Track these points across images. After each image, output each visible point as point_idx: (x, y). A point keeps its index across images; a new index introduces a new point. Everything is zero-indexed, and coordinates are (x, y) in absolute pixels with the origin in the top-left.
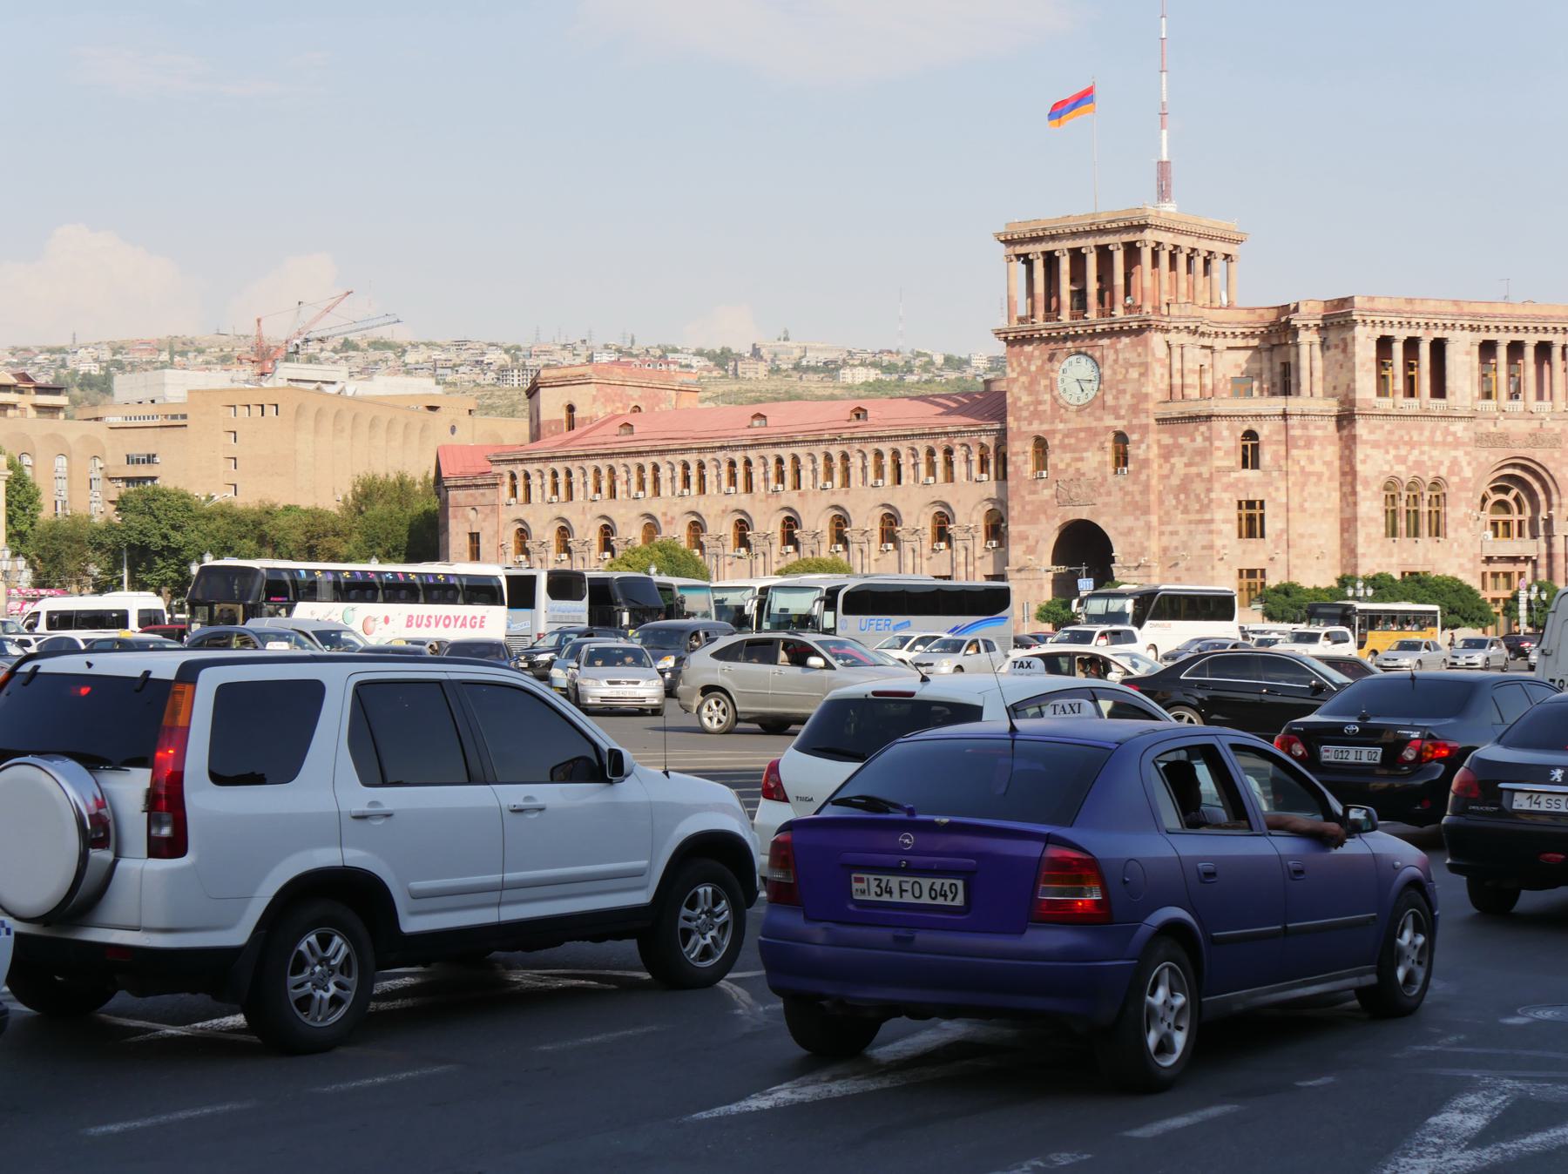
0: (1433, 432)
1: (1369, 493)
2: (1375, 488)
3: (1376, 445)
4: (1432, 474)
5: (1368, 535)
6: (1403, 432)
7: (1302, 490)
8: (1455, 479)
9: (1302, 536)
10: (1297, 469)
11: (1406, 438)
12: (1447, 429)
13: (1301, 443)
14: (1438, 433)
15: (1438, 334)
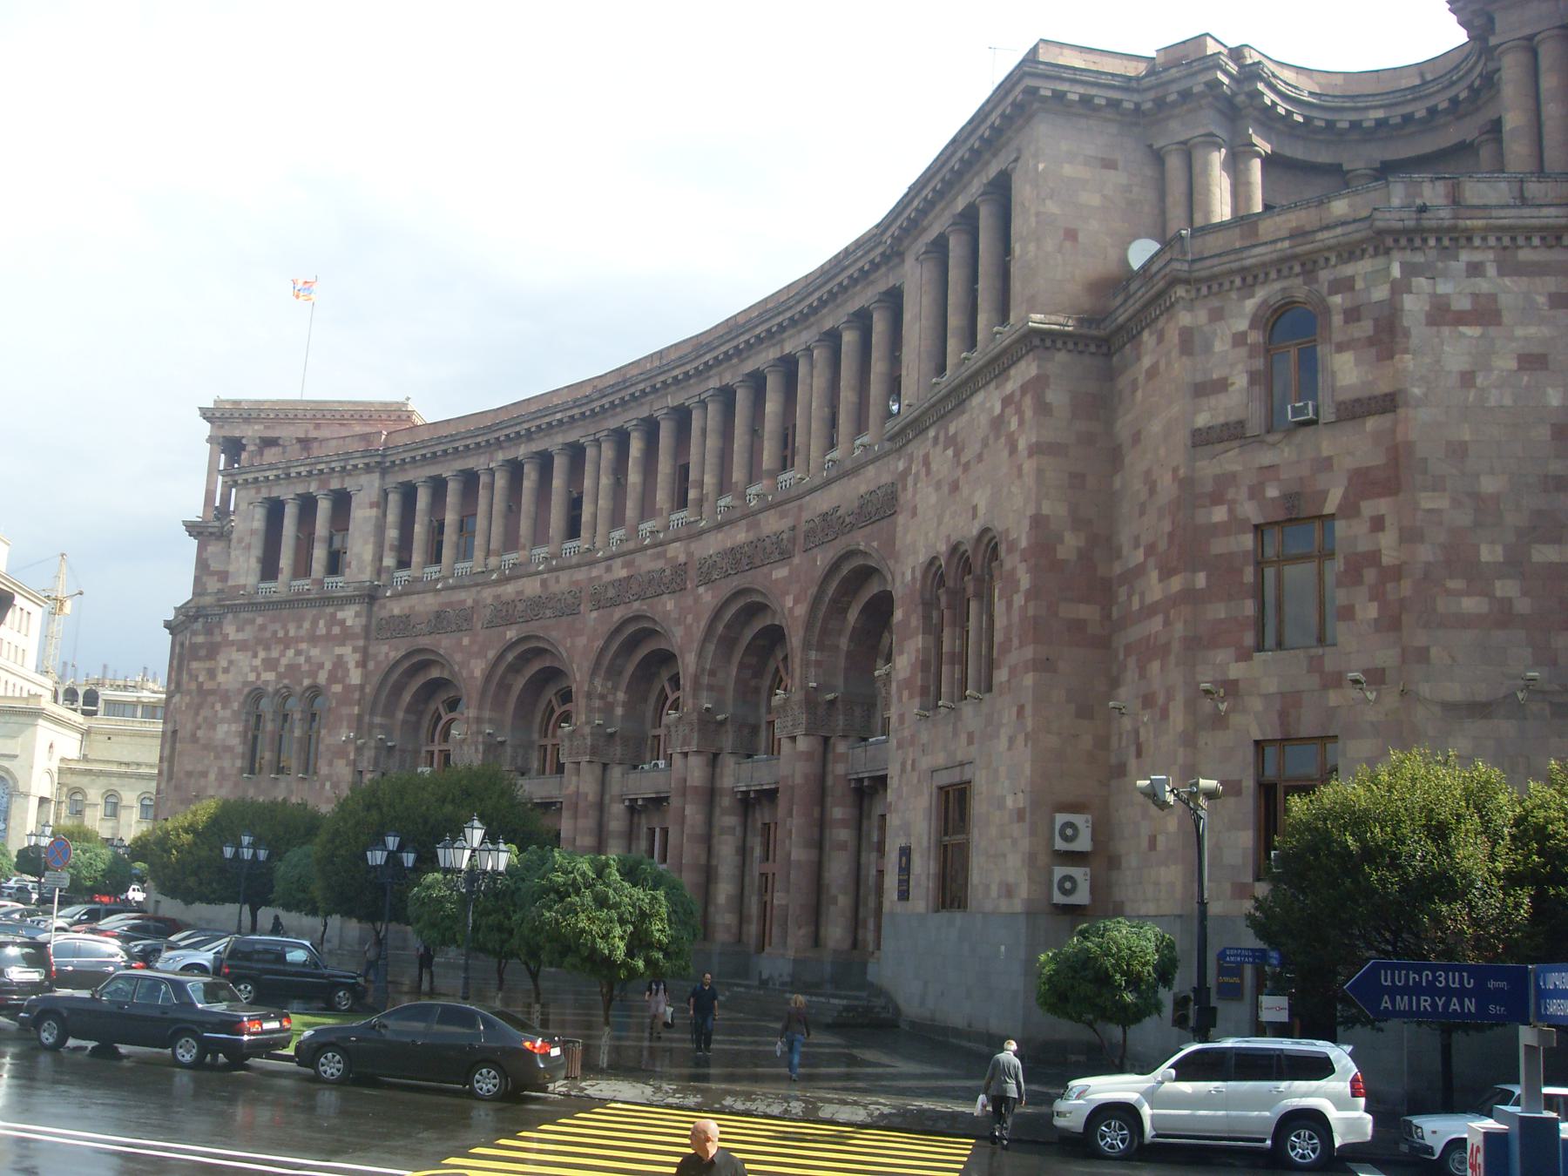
0: (315, 623)
1: (228, 713)
2: (236, 706)
3: (243, 646)
4: (306, 682)
5: (221, 769)
6: (277, 626)
7: (197, 714)
8: (337, 688)
9: (189, 774)
10: (193, 686)
11: (281, 634)
12: (333, 615)
13: (203, 653)
14: (321, 623)
15: (335, 484)
